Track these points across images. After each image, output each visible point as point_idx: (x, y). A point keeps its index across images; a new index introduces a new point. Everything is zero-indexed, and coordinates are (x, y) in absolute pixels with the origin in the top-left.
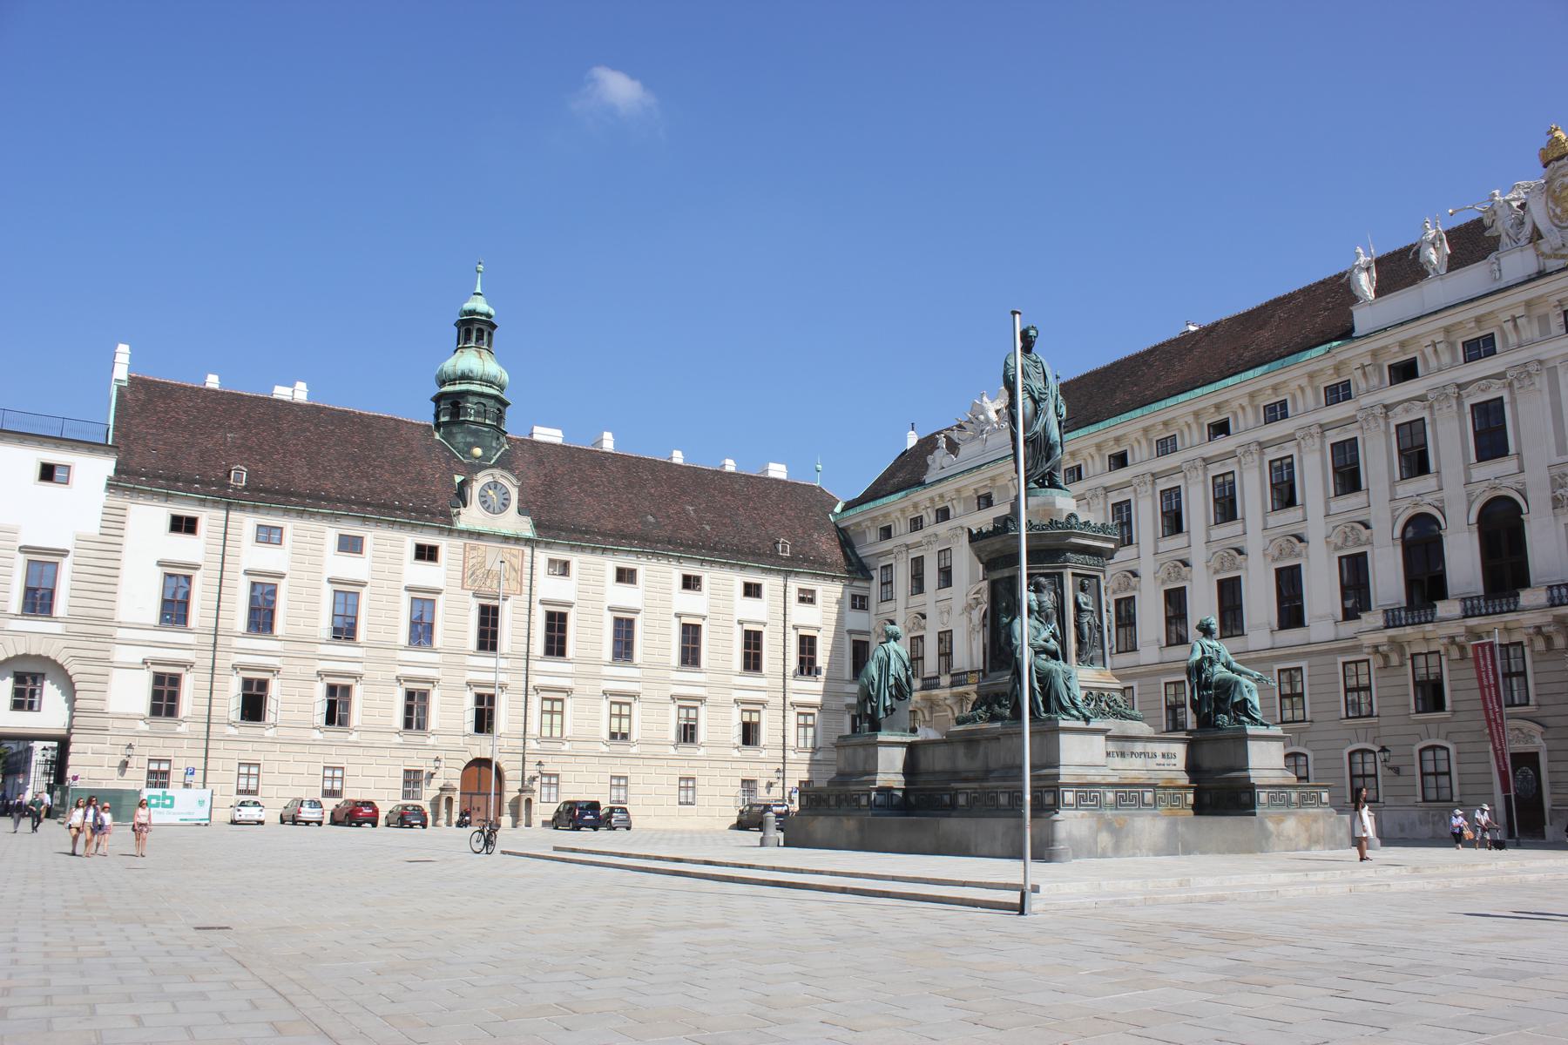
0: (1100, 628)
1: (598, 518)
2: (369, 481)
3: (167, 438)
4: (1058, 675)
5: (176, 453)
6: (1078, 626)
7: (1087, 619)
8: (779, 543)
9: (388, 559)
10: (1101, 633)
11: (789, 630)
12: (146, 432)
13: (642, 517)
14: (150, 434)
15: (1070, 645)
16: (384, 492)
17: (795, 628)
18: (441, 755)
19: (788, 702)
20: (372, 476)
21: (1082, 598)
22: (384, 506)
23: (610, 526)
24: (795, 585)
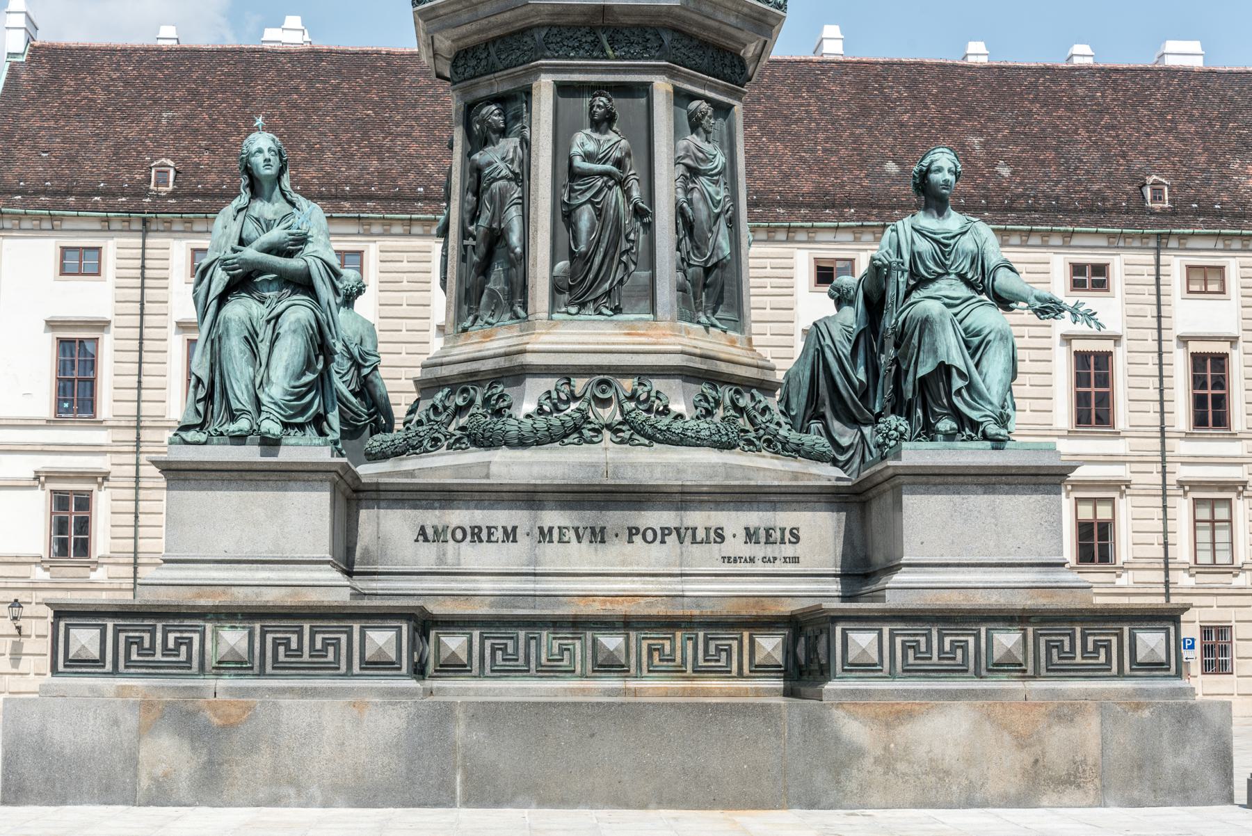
0: (643, 214)
1: (786, 177)
2: (381, 160)
3: (70, 131)
4: (227, 330)
5: (78, 151)
6: (566, 215)
7: (588, 195)
8: (1145, 185)
9: (405, 283)
10: (649, 227)
11: (1170, 345)
12: (40, 128)
13: (873, 167)
14: (45, 128)
15: (535, 265)
16: (405, 172)
17: (1184, 340)
18: (22, 597)
19: (1171, 479)
20: (389, 150)
21: (584, 141)
22: (397, 197)
23: (807, 187)
24: (1175, 264)
